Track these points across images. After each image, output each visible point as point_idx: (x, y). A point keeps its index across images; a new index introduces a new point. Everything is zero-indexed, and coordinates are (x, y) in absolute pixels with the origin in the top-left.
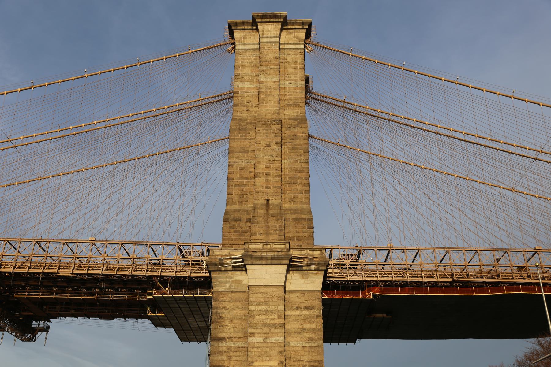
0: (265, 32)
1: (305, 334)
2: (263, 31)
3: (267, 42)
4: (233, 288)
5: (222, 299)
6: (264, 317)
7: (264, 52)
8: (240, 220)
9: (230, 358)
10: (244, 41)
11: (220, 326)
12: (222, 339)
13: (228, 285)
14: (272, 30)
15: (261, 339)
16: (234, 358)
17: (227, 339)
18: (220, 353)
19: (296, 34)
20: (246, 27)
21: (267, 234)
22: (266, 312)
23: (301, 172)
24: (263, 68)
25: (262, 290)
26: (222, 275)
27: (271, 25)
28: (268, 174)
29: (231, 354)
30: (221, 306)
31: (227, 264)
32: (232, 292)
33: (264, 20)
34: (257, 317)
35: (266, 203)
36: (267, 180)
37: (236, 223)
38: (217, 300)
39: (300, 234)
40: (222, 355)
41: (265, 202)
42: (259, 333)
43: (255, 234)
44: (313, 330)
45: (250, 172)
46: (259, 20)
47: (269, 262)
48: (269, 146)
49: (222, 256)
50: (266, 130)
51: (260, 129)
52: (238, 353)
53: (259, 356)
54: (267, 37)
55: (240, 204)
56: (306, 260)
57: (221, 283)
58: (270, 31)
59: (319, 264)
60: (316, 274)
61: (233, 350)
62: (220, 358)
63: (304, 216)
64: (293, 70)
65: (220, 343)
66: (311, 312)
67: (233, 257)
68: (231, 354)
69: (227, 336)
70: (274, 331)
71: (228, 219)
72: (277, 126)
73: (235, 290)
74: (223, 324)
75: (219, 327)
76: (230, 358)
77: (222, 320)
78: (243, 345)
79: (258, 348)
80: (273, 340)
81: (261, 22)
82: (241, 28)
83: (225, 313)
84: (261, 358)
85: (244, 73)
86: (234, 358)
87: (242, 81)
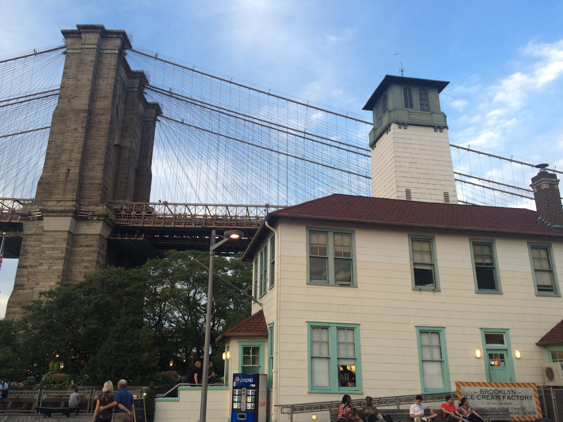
0: (87, 40)
1: (83, 264)
2: (85, 39)
3: (87, 48)
4: (38, 232)
6: (51, 252)
8: (50, 184)
9: (29, 279)
13: (34, 230)
15: (46, 267)
17: (29, 267)
20: (75, 36)
21: (64, 194)
22: (53, 249)
23: (100, 149)
24: (81, 69)
25: (52, 234)
26: (31, 223)
31: (34, 215)
32: (37, 235)
33: (86, 30)
35: (67, 172)
36: (70, 155)
37: (46, 186)
38: (26, 241)
39: (92, 195)
40: (24, 277)
41: (67, 171)
42: (46, 263)
44: (89, 261)
46: (82, 31)
47: (59, 214)
48: (76, 129)
49: (31, 209)
50: (76, 117)
51: (71, 116)
53: (43, 279)
54: (88, 44)
55: (53, 171)
56: (90, 213)
59: (99, 216)
60: (97, 222)
62: (22, 279)
63: (96, 181)
64: (107, 71)
65: (24, 269)
66: (90, 248)
69: (29, 264)
70: (56, 261)
71: (42, 183)
72: (84, 114)
73: (39, 233)
74: (27, 256)
76: (29, 279)
77: (27, 254)
79: (43, 273)
80: (54, 267)
81: (84, 32)
84: (44, 280)
86: (32, 279)
87: (68, 78)
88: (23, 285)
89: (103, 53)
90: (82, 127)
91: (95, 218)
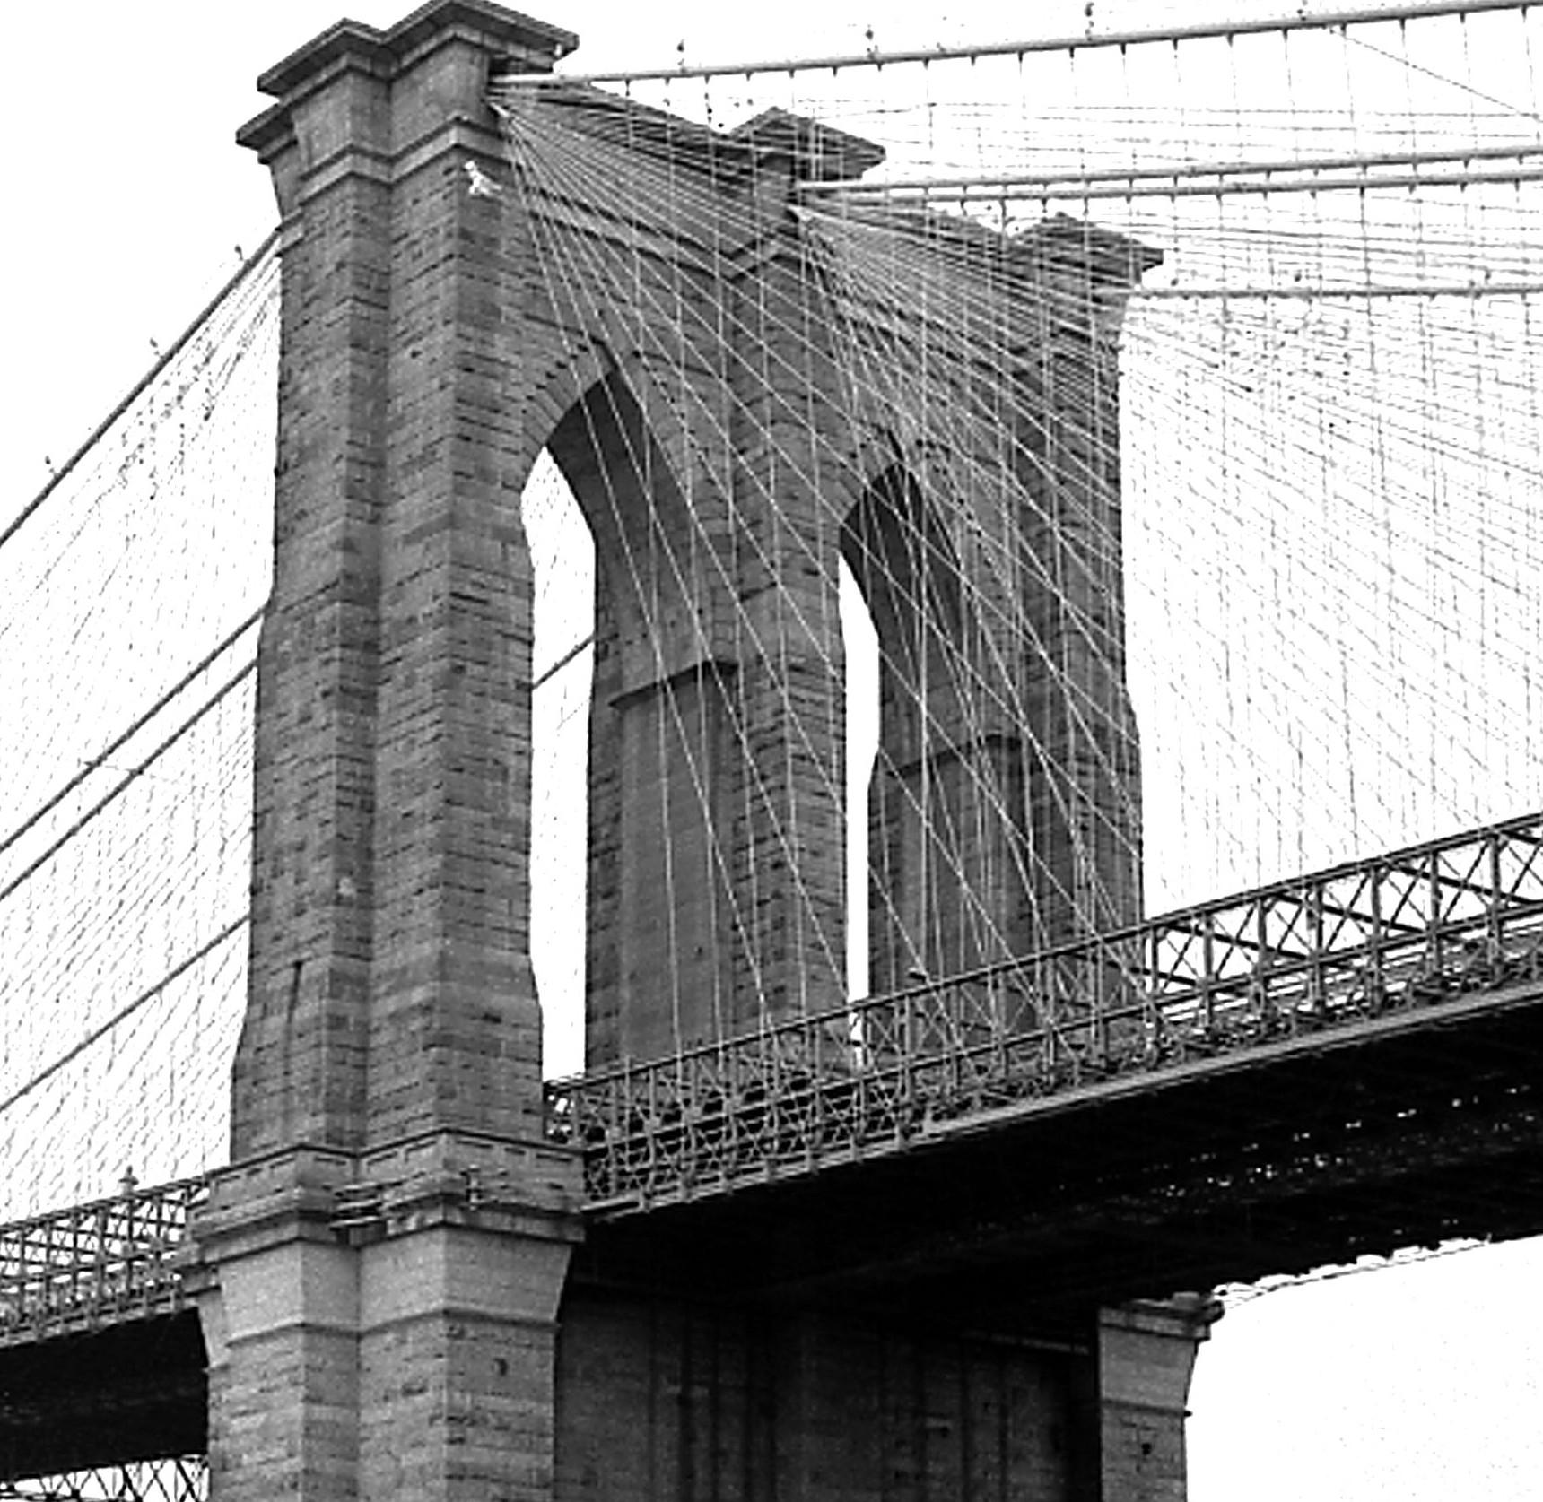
28: (301, 848)
48: (306, 718)
54: (319, 169)
63: (418, 995)
89: (400, 181)
90: (325, 694)
91: (411, 1224)
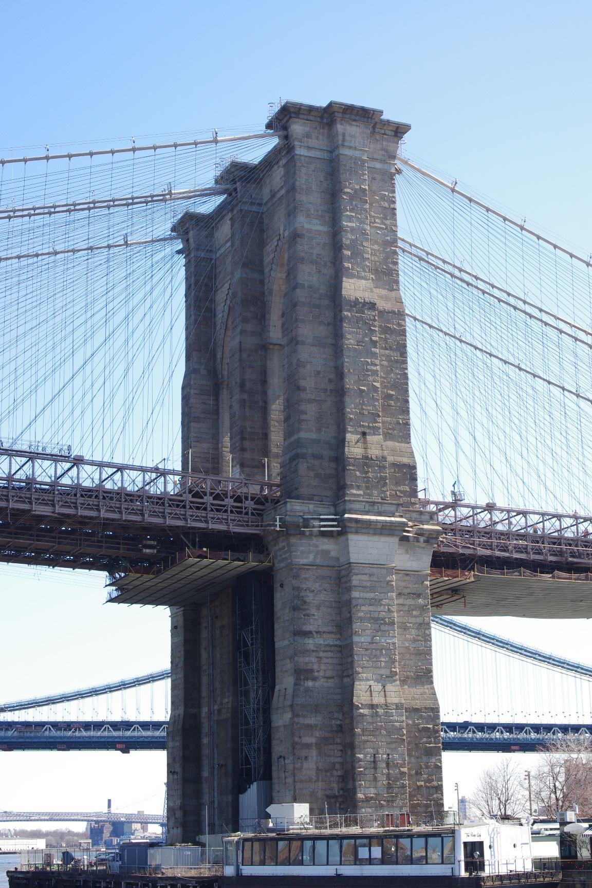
0: (347, 138)
2: (344, 135)
5: (305, 576)
7: (346, 174)
10: (308, 142)
11: (304, 615)
12: (308, 634)
14: (357, 135)
16: (324, 660)
18: (306, 652)
19: (384, 143)
27: (357, 126)
29: (321, 654)
30: (304, 586)
34: (363, 608)
40: (309, 656)
43: (352, 487)
45: (329, 379)
52: (330, 653)
57: (302, 552)
58: (353, 136)
61: (323, 649)
62: (307, 659)
67: (322, 517)
68: (321, 654)
69: (315, 629)
74: (308, 612)
75: (303, 617)
78: (335, 643)
82: (306, 117)
83: (310, 597)
85: (310, 203)
86: (324, 660)
88: (312, 671)
